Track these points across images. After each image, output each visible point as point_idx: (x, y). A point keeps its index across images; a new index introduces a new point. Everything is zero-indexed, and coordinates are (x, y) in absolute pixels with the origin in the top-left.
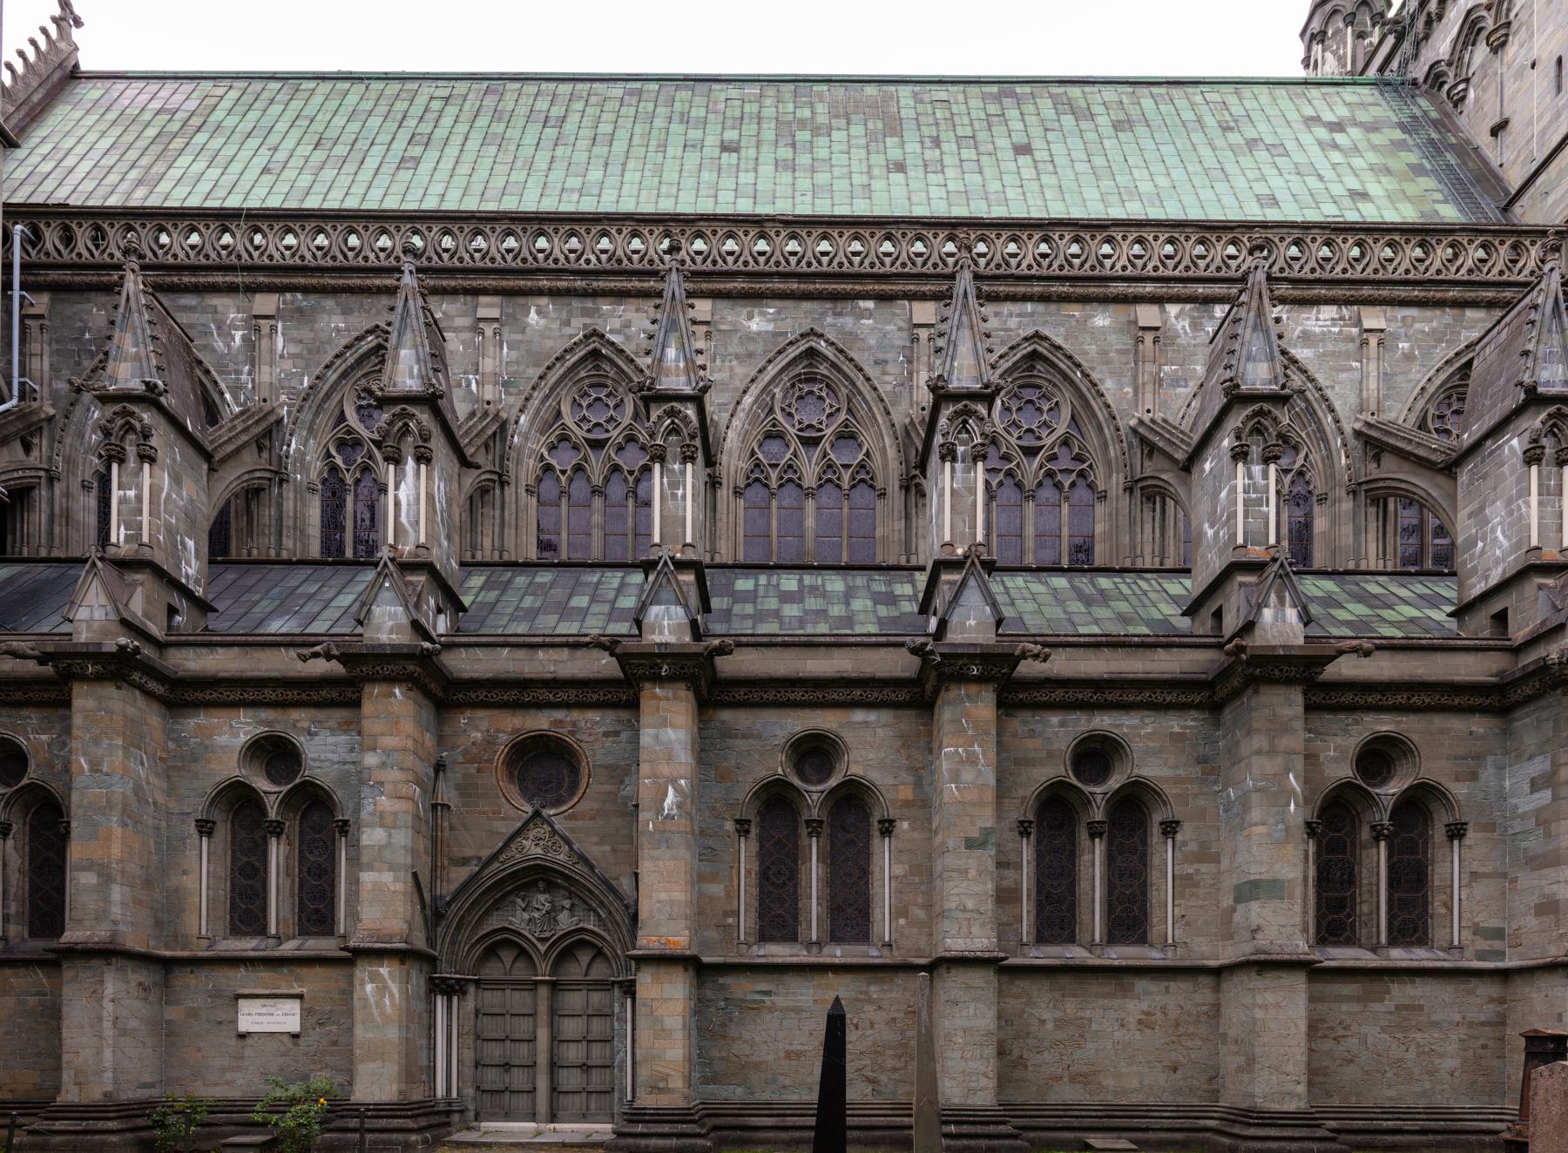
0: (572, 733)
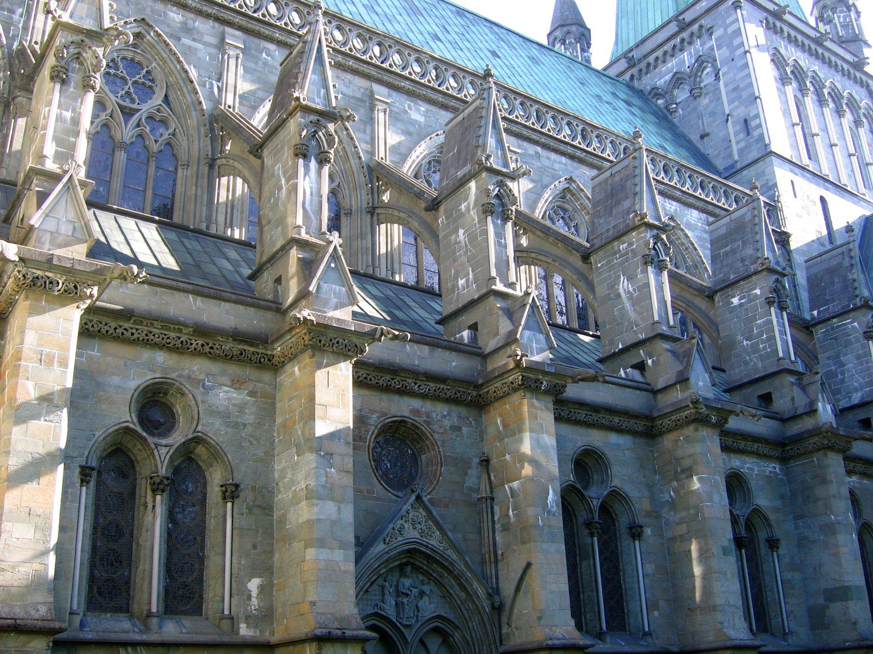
0: (427, 423)
